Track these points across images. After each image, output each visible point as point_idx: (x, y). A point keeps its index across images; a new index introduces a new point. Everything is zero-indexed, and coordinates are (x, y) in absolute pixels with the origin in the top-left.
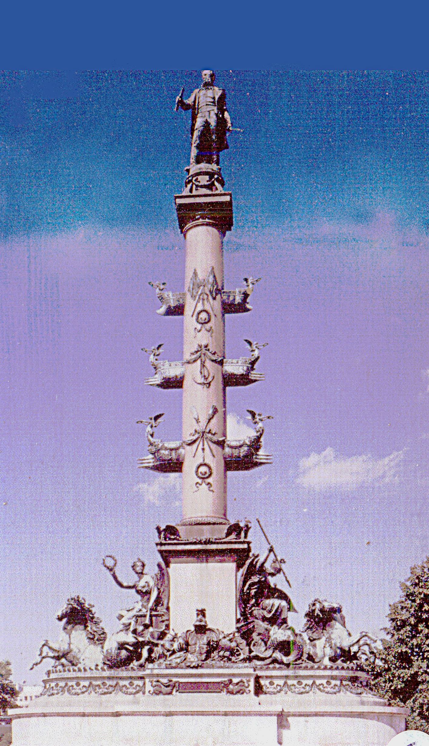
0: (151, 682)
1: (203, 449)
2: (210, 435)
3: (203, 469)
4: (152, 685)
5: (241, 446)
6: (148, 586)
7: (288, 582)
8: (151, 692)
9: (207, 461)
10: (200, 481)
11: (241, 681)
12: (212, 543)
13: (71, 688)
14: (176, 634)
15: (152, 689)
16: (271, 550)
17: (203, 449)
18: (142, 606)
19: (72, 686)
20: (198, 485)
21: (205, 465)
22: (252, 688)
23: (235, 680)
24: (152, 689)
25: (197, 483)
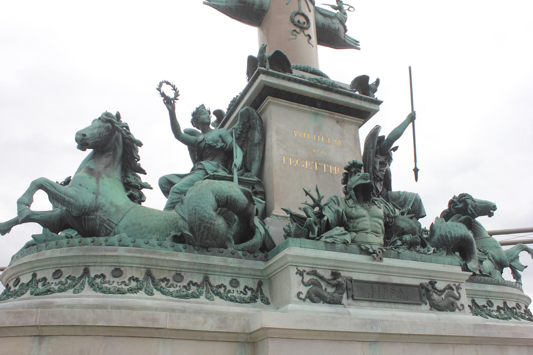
0: (301, 273)
4: (303, 282)
6: (223, 141)
7: (416, 170)
8: (302, 296)
10: (298, 30)
11: (450, 288)
12: (337, 92)
13: (98, 280)
14: (320, 198)
15: (305, 290)
16: (412, 118)
18: (218, 167)
19: (103, 276)
20: (295, 33)
22: (465, 300)
23: (440, 285)
24: (305, 290)
25: (295, 31)
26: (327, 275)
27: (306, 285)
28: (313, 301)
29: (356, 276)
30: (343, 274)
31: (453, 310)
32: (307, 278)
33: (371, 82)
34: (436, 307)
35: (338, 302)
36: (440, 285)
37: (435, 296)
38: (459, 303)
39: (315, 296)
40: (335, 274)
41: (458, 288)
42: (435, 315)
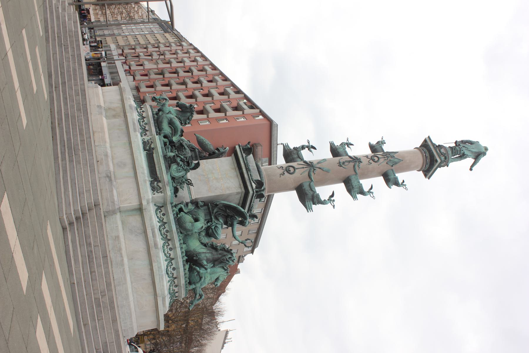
0: (151, 139)
1: (303, 168)
2: (312, 170)
3: (292, 170)
5: (312, 190)
9: (297, 170)
10: (284, 168)
15: (146, 140)
17: (303, 168)
21: (295, 170)
23: (160, 184)
26: (152, 146)
27: (148, 141)
28: (143, 143)
29: (154, 155)
30: (154, 151)
31: (152, 190)
32: (150, 141)
33: (263, 188)
34: (152, 183)
35: (145, 149)
36: (160, 184)
37: (156, 183)
38: (155, 192)
39: (144, 143)
40: (153, 149)
41: (161, 192)
42: (148, 184)
